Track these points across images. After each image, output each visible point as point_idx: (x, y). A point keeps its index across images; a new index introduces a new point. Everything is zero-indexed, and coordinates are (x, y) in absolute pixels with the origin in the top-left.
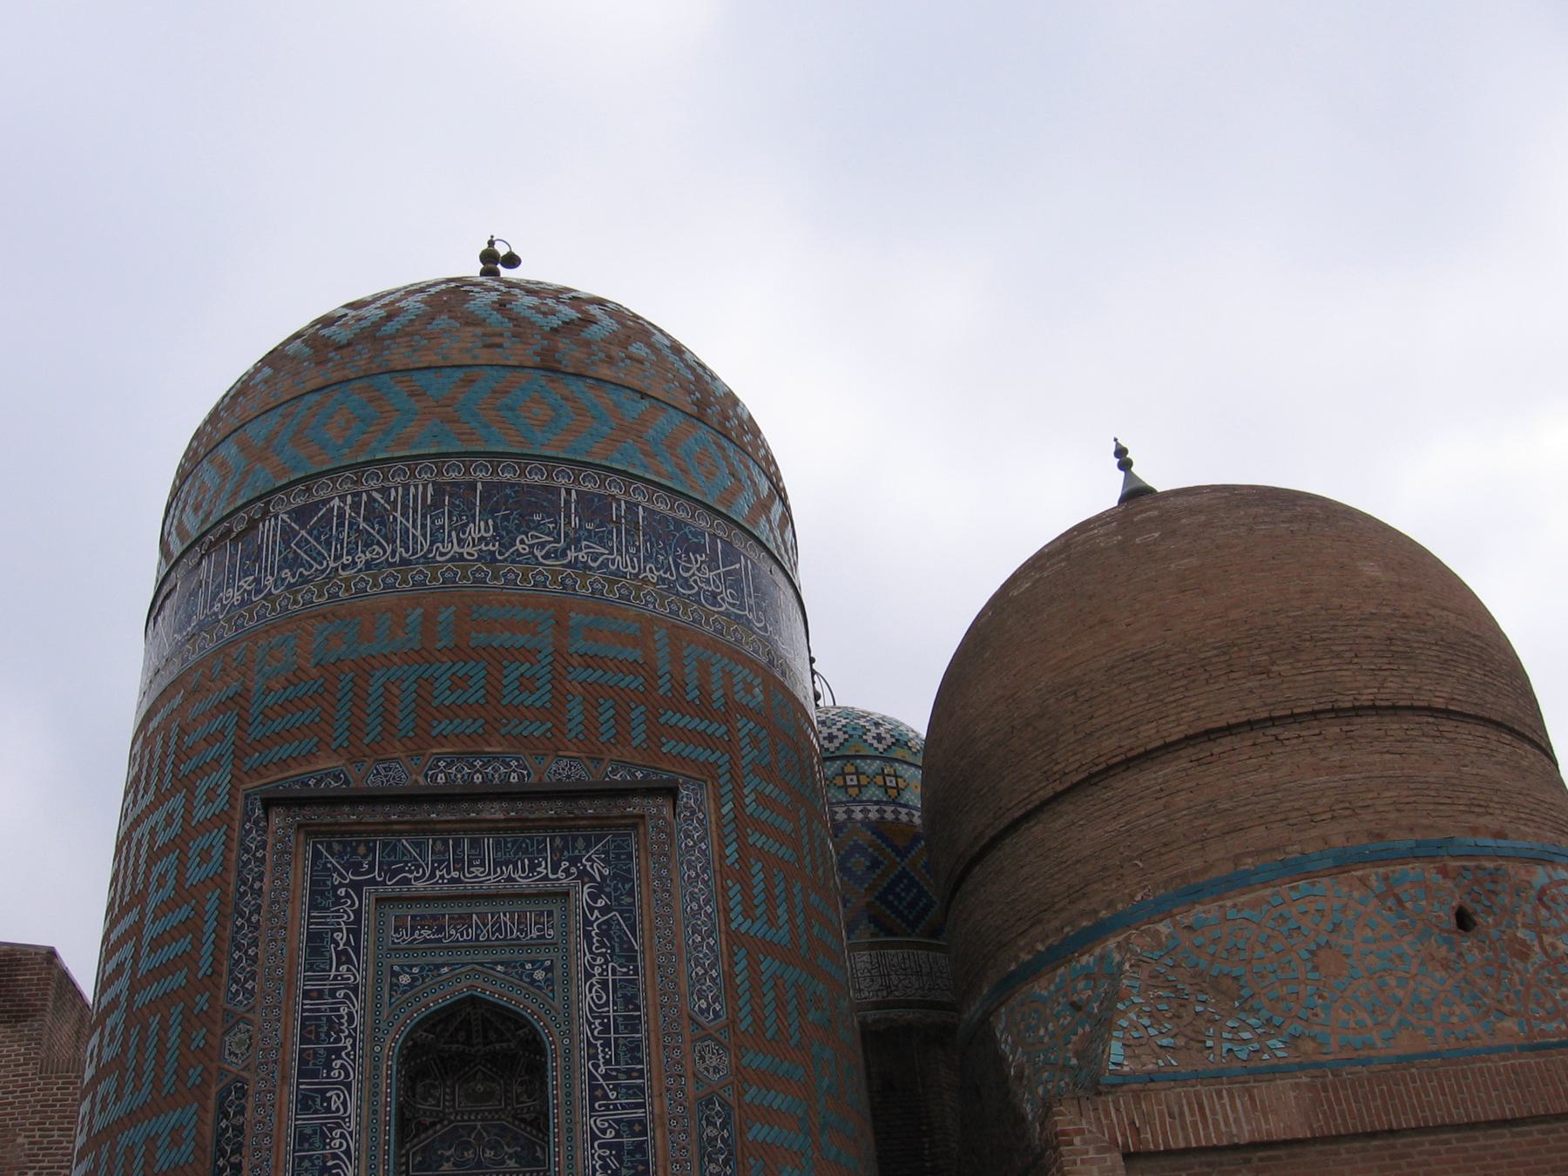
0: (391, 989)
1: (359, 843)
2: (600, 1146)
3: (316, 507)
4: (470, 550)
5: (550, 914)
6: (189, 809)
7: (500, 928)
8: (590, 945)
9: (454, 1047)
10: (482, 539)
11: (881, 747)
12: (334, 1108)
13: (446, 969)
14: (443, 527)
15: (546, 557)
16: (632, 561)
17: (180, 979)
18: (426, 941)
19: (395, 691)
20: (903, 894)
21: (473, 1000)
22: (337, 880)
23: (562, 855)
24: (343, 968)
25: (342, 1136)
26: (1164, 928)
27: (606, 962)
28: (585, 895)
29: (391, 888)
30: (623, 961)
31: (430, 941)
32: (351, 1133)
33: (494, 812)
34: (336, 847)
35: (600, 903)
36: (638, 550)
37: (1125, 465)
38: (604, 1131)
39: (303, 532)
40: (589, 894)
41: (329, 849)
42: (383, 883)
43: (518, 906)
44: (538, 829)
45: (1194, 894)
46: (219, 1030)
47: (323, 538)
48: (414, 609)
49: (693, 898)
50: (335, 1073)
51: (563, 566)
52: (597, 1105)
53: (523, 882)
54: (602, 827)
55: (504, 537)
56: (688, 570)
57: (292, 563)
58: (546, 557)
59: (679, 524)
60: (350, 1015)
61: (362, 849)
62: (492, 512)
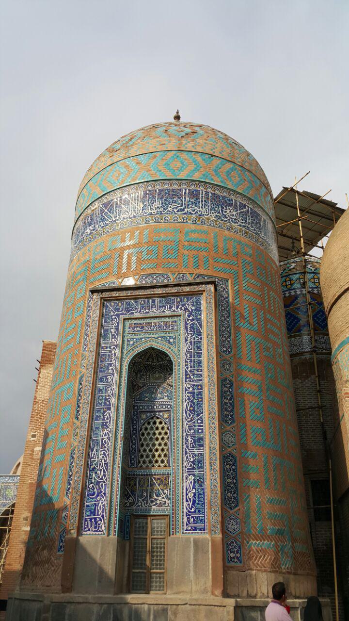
0: (127, 346)
1: (119, 303)
2: (188, 393)
3: (109, 202)
4: (154, 211)
5: (176, 322)
7: (160, 327)
8: (187, 331)
9: (148, 363)
10: (158, 207)
11: (313, 269)
12: (109, 381)
13: (144, 339)
14: (146, 205)
15: (178, 211)
16: (206, 210)
18: (138, 331)
19: (131, 256)
20: (320, 317)
21: (152, 348)
22: (112, 314)
23: (179, 302)
24: (114, 339)
25: (111, 389)
27: (192, 336)
28: (186, 316)
29: (128, 316)
30: (197, 335)
31: (139, 331)
32: (114, 389)
34: (112, 304)
35: (191, 318)
36: (209, 206)
38: (189, 388)
39: (106, 210)
40: (188, 315)
41: (110, 305)
42: (126, 314)
43: (166, 320)
44: (172, 296)
46: (80, 359)
47: (111, 211)
48: (137, 231)
49: (223, 316)
50: (110, 371)
51: (184, 214)
52: (187, 380)
53: (168, 313)
54: (192, 295)
55: (165, 206)
56: (226, 212)
58: (178, 211)
59: (224, 197)
60: (115, 353)
61: (120, 304)
62: (161, 198)
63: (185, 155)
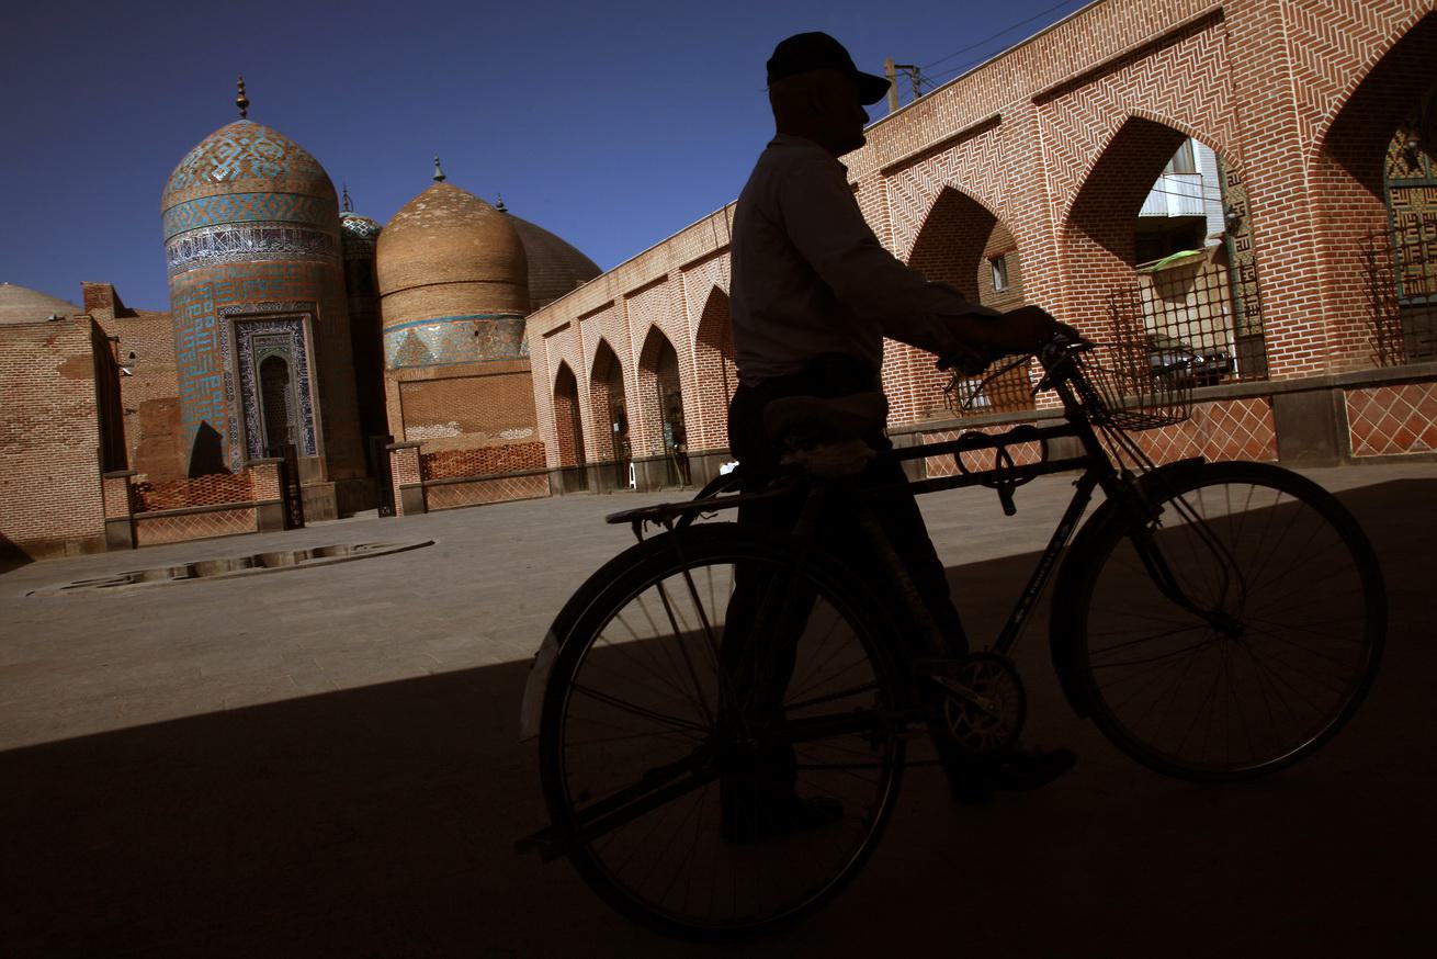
3: (222, 233)
6: (203, 310)
17: (209, 348)
26: (416, 329)
33: (274, 317)
45: (423, 322)
55: (269, 244)
57: (218, 249)
63: (280, 197)
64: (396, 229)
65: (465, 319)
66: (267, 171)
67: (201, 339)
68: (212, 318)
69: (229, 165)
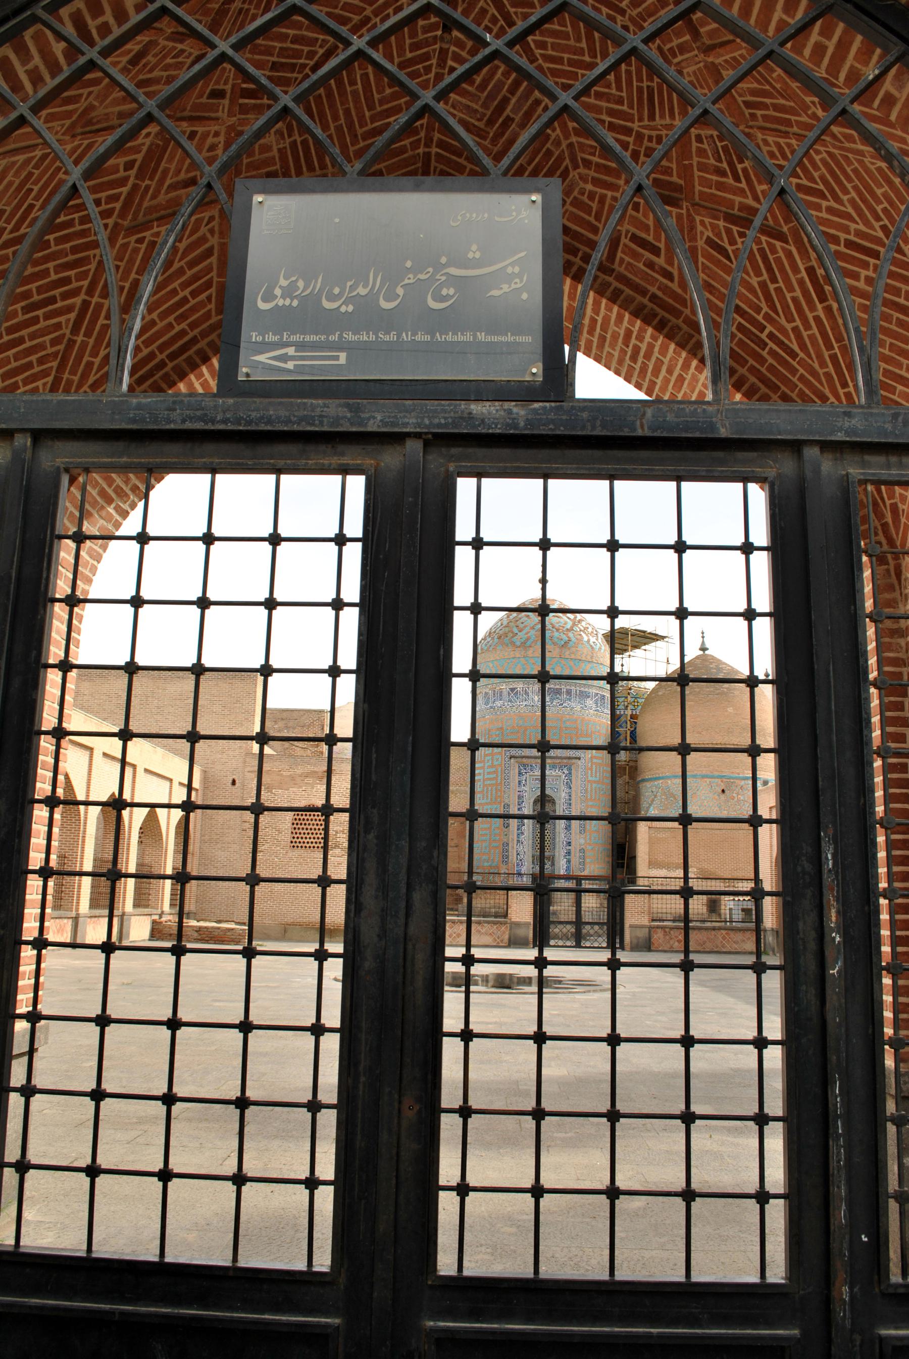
3: (514, 689)
17: (494, 782)
37: (703, 637)
57: (511, 701)
64: (660, 693)
65: (713, 777)
66: (556, 640)
67: (489, 773)
68: (499, 757)
69: (526, 634)
